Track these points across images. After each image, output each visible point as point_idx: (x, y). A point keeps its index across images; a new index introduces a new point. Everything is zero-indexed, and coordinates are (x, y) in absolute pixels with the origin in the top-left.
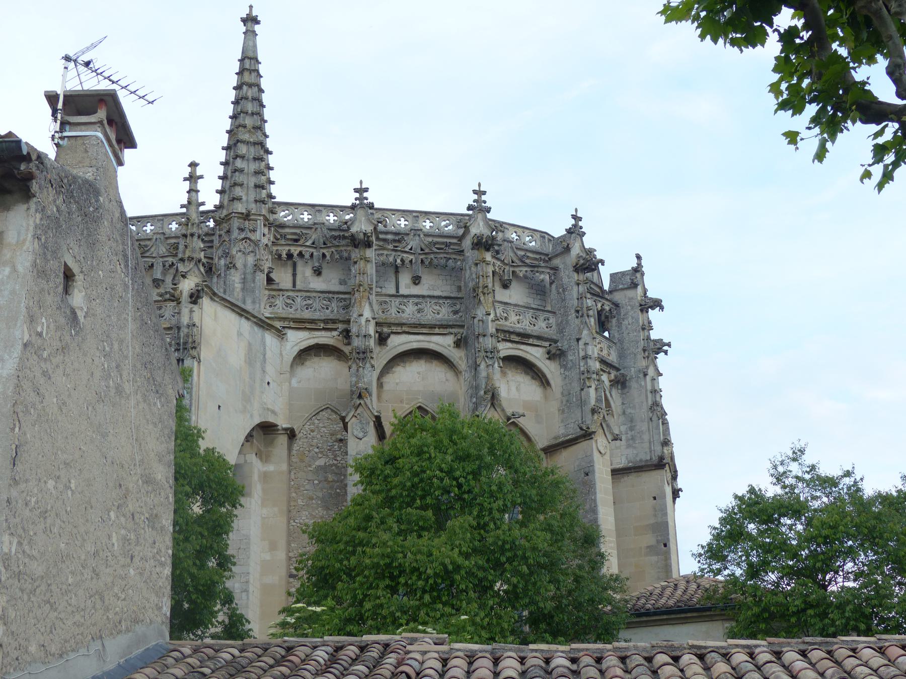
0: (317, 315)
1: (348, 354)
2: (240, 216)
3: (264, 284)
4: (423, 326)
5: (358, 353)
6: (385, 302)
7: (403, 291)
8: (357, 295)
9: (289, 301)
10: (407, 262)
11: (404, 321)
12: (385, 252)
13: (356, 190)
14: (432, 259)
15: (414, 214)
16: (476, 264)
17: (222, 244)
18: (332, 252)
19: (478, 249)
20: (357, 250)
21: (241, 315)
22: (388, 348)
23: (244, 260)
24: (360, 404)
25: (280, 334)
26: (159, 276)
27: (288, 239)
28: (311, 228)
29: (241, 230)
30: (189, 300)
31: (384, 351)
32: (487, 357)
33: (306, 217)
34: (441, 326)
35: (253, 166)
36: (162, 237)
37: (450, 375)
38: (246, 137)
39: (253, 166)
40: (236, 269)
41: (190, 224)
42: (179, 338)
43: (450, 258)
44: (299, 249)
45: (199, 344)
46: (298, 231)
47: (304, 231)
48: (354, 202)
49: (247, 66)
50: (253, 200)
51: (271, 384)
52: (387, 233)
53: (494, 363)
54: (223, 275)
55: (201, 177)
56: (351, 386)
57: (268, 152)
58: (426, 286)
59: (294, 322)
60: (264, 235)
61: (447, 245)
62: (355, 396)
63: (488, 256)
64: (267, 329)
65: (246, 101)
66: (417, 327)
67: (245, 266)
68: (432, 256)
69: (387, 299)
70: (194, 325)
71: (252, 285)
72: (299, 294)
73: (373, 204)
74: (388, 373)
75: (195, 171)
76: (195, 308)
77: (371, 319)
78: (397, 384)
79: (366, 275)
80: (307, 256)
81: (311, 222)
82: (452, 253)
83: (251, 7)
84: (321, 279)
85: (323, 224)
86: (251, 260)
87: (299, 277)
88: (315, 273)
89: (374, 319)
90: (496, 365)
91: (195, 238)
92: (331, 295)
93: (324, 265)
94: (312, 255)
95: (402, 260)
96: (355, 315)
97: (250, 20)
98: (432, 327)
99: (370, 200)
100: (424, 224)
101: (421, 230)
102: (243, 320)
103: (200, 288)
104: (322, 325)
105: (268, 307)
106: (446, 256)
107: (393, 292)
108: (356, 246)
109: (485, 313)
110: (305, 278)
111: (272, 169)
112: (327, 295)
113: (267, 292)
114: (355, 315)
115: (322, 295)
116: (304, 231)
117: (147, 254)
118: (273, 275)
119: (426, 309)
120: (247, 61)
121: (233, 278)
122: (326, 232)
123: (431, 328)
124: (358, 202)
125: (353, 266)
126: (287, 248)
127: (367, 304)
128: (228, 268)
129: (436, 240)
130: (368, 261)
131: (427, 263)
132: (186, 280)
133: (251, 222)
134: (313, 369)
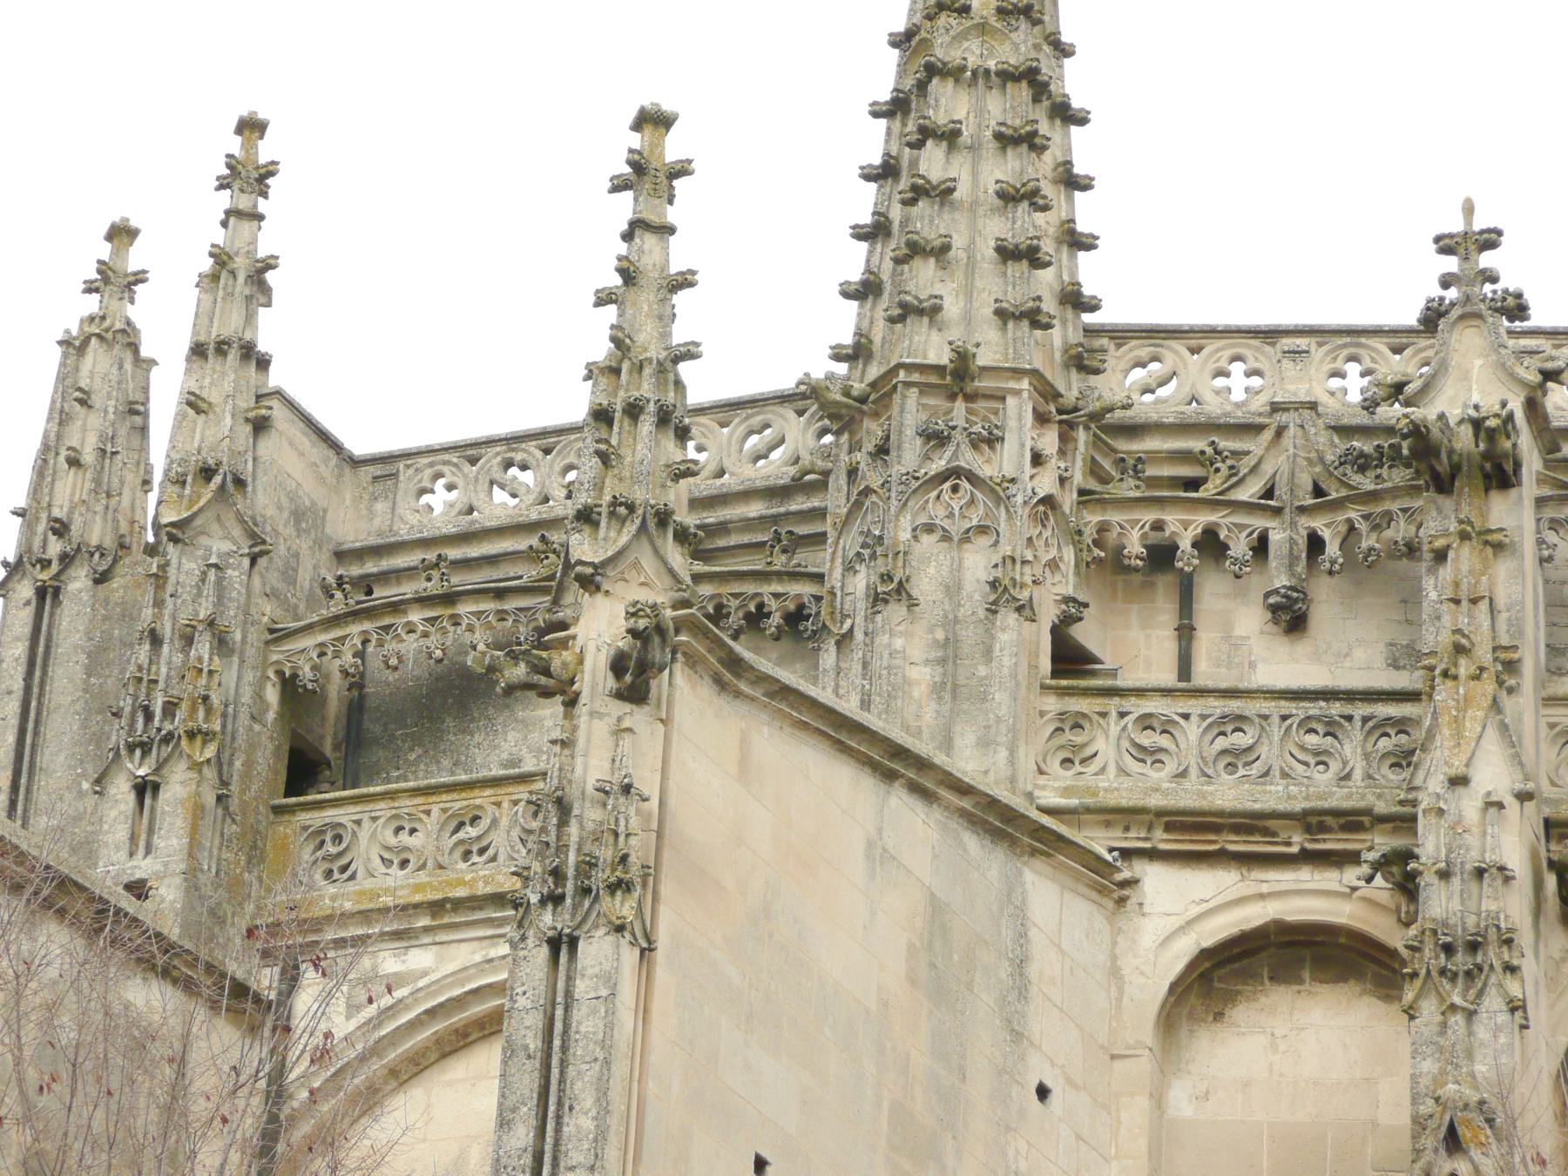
0: (1273, 796)
1: (1404, 953)
2: (933, 379)
3: (1034, 667)
5: (1448, 949)
8: (1443, 692)
9: (1147, 739)
13: (1446, 245)
17: (858, 505)
18: (1352, 528)
20: (1447, 503)
21: (889, 776)
27: (1154, 482)
29: (936, 438)
30: (611, 683)
33: (1238, 383)
38: (972, 53)
40: (912, 604)
41: (625, 367)
42: (562, 849)
44: (1204, 518)
45: (650, 874)
46: (1197, 444)
47: (1225, 444)
48: (1437, 291)
50: (988, 311)
51: (1055, 1099)
54: (859, 635)
55: (682, 170)
56: (1415, 1099)
57: (1067, 115)
59: (1168, 828)
62: (1430, 1141)
64: (1034, 852)
67: (953, 589)
70: (627, 789)
71: (982, 671)
72: (1194, 706)
73: (1519, 296)
75: (658, 145)
76: (638, 717)
77: (1509, 800)
79: (1484, 606)
80: (1240, 547)
81: (1259, 403)
84: (1303, 647)
85: (1313, 406)
86: (978, 563)
88: (1276, 621)
89: (1523, 797)
91: (647, 424)
92: (1336, 709)
94: (1261, 547)
96: (1436, 784)
99: (1508, 282)
102: (899, 800)
103: (642, 623)
104: (1298, 841)
105: (1054, 766)
108: (1443, 484)
110: (1234, 644)
111: (1083, 184)
112: (1315, 709)
113: (1052, 704)
114: (1436, 784)
115: (1299, 710)
116: (1225, 444)
118: (1086, 634)
121: (899, 643)
122: (1322, 439)
124: (1452, 294)
125: (1432, 571)
126: (1149, 516)
127: (1492, 734)
128: (877, 600)
130: (1498, 547)
132: (599, 597)
133: (980, 405)
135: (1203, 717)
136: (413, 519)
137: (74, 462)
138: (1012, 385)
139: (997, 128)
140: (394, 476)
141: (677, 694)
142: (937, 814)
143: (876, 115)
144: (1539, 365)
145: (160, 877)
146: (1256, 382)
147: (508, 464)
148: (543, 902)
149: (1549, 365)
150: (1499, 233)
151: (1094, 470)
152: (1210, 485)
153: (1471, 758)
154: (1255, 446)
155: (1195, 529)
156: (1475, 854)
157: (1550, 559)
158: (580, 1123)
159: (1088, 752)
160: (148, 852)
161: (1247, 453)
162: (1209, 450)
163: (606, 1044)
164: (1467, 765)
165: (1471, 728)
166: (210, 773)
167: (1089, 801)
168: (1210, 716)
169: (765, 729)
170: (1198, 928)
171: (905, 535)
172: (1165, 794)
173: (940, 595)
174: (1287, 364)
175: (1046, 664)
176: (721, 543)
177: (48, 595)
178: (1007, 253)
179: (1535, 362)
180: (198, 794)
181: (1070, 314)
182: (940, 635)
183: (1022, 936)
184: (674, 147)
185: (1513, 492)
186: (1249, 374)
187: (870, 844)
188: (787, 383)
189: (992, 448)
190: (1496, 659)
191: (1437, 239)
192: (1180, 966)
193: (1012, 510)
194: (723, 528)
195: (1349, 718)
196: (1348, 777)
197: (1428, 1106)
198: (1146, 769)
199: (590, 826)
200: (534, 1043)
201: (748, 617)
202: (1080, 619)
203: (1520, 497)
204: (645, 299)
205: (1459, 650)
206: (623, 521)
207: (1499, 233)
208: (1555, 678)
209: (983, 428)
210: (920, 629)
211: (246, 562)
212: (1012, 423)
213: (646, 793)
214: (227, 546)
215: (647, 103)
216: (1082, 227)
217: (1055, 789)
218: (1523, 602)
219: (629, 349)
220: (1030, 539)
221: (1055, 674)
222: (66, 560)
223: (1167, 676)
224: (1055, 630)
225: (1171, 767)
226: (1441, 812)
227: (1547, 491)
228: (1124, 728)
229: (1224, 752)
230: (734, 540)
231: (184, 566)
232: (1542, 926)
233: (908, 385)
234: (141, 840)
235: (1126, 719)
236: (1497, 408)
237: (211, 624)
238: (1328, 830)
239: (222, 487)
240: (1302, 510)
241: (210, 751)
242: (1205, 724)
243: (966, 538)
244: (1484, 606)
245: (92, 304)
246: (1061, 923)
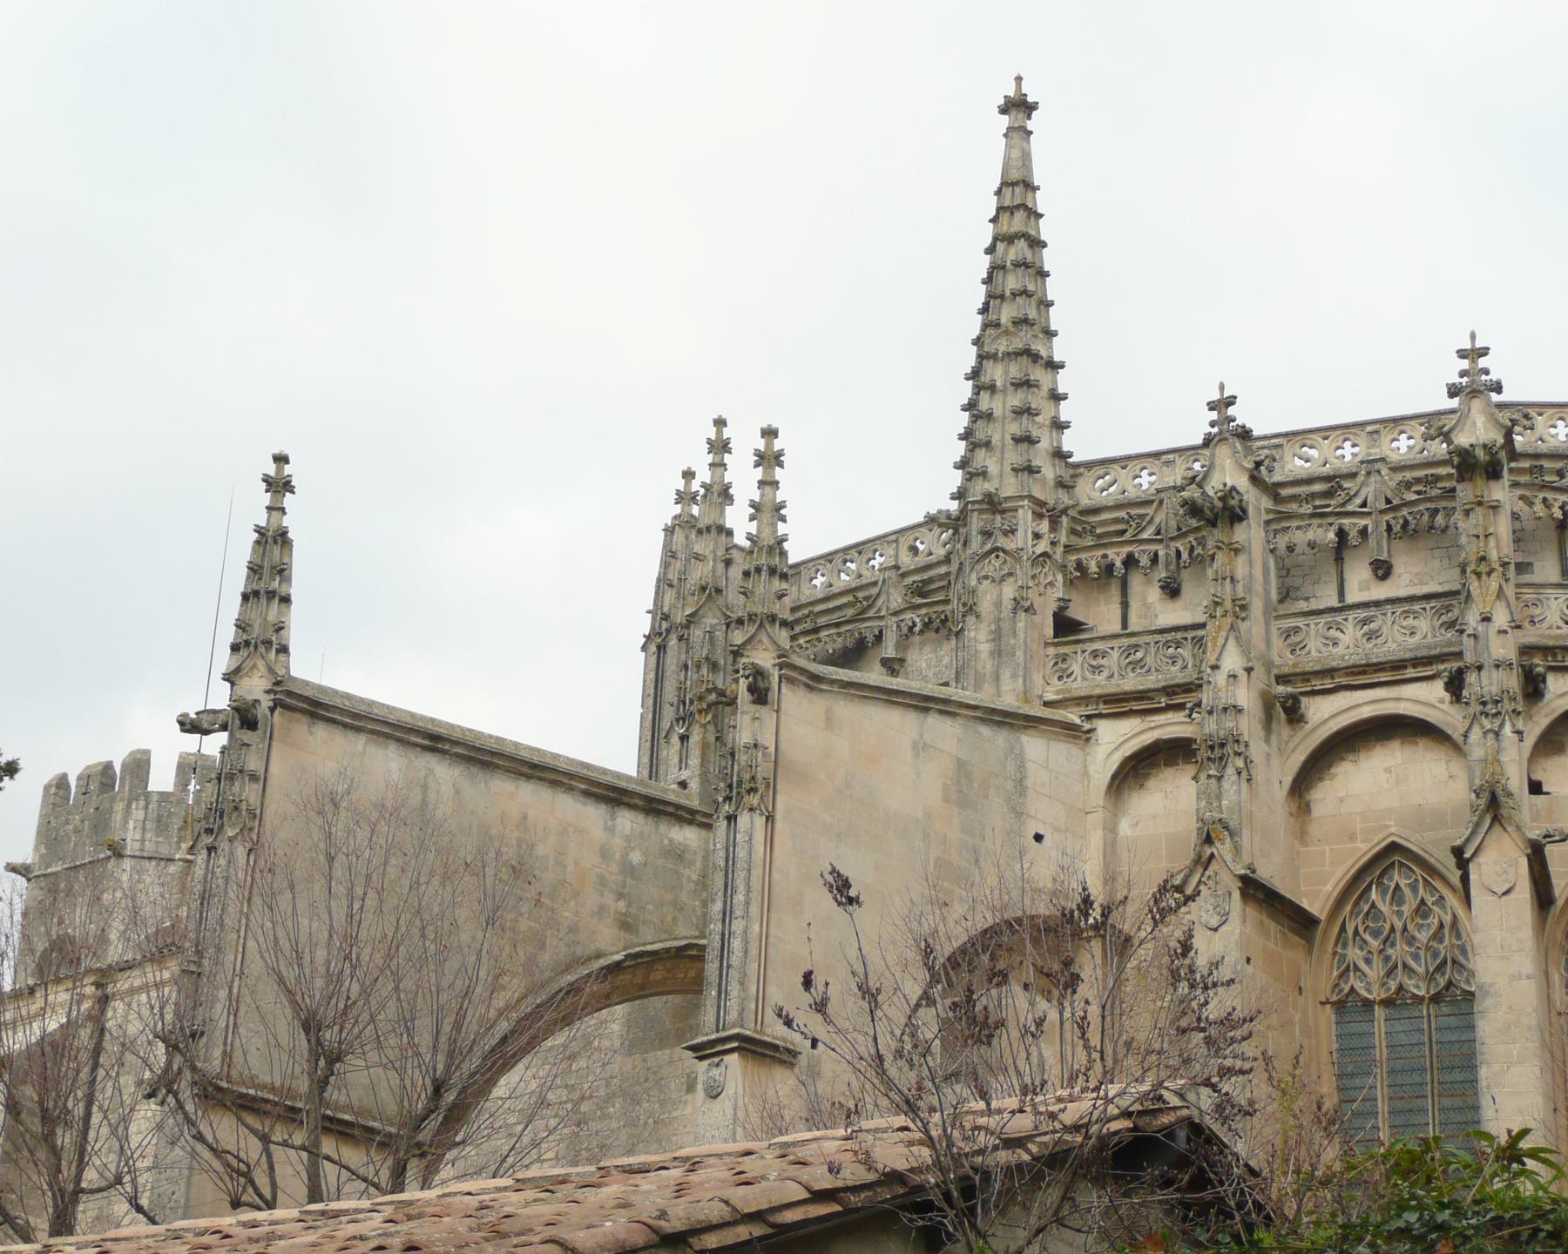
0: (1151, 681)
2: (985, 506)
4: (1379, 667)
5: (1212, 748)
6: (1297, 630)
7: (1353, 597)
10: (1353, 534)
11: (1334, 664)
12: (1295, 523)
13: (1212, 406)
14: (1406, 522)
15: (1369, 428)
16: (1467, 513)
19: (1471, 480)
20: (1215, 531)
21: (926, 710)
22: (1308, 727)
23: (993, 597)
24: (1212, 855)
25: (1079, 735)
26: (889, 650)
27: (1099, 536)
28: (1153, 501)
30: (750, 698)
31: (1300, 734)
32: (1487, 715)
33: (1145, 480)
34: (1417, 662)
35: (1016, 399)
36: (893, 574)
37: (1456, 767)
39: (1016, 399)
40: (978, 617)
43: (1436, 511)
45: (771, 785)
46: (1122, 514)
47: (1134, 512)
49: (1007, 203)
52: (1309, 481)
53: (1502, 725)
57: (1054, 366)
58: (1405, 579)
59: (1105, 703)
60: (1037, 536)
61: (1438, 478)
63: (1500, 492)
64: (1026, 727)
65: (1001, 272)
66: (1364, 672)
67: (998, 604)
68: (1405, 512)
69: (1300, 622)
70: (756, 746)
72: (1116, 643)
73: (1244, 427)
74: (1320, 780)
76: (763, 711)
78: (1341, 800)
80: (1144, 561)
81: (1153, 490)
82: (1439, 498)
83: (1019, 79)
84: (1179, 603)
86: (1009, 591)
87: (1134, 605)
90: (1508, 729)
92: (1179, 635)
93: (1185, 575)
94: (1155, 560)
95: (1341, 534)
97: (1019, 106)
98: (1399, 665)
99: (1239, 422)
100: (1395, 444)
101: (1383, 460)
102: (933, 720)
104: (1164, 701)
106: (1429, 505)
107: (1334, 603)
108: (1213, 523)
109: (1479, 618)
110: (1146, 606)
112: (1169, 637)
113: (1051, 651)
116: (1134, 512)
117: (871, 614)
118: (1076, 612)
119: (1384, 629)
120: (1008, 192)
123: (1395, 670)
124: (1215, 430)
125: (1211, 566)
126: (1099, 553)
127: (1232, 641)
129: (1409, 475)
131: (1397, 528)
134: (1162, 795)
136: (807, 592)
137: (671, 586)
138: (1021, 503)
140: (800, 573)
141: (783, 698)
142: (959, 720)
143: (967, 379)
145: (691, 778)
146: (1153, 478)
147: (845, 561)
148: (725, 800)
149: (1258, 459)
150: (1235, 397)
151: (1073, 532)
154: (1150, 511)
156: (1223, 701)
157: (1275, 549)
158: (739, 898)
159: (1069, 671)
162: (1126, 517)
163: (749, 862)
164: (1218, 659)
165: (1221, 641)
166: (711, 728)
167: (1067, 695)
169: (842, 703)
170: (1123, 747)
171: (974, 583)
173: (992, 609)
174: (1165, 468)
175: (1050, 632)
176: (932, 587)
177: (661, 649)
178: (1017, 440)
179: (1253, 458)
180: (704, 738)
181: (1057, 461)
182: (993, 627)
183: (1021, 767)
184: (778, 445)
185: (1245, 522)
186: (1151, 474)
187: (915, 745)
188: (921, 519)
191: (1208, 404)
192: (1115, 767)
194: (931, 580)
195: (1186, 639)
196: (1186, 667)
197: (1200, 824)
199: (743, 763)
200: (723, 864)
201: (942, 621)
203: (1249, 526)
204: (766, 516)
205: (1217, 604)
206: (755, 622)
207: (1235, 397)
210: (983, 626)
211: (724, 627)
212: (1021, 522)
213: (767, 744)
214: (715, 621)
215: (765, 426)
216: (1063, 418)
218: (1251, 575)
220: (1034, 577)
221: (1056, 636)
222: (668, 631)
223: (1116, 627)
224: (1056, 615)
225: (1105, 674)
226: (1209, 682)
227: (1272, 516)
229: (1130, 663)
230: (937, 585)
231: (697, 633)
232: (1274, 726)
233: (973, 511)
234: (683, 763)
236: (1221, 487)
237: (707, 659)
238: (1178, 694)
239: (710, 594)
240: (1172, 539)
241: (709, 718)
243: (1002, 580)
244: (1228, 580)
245: (678, 509)
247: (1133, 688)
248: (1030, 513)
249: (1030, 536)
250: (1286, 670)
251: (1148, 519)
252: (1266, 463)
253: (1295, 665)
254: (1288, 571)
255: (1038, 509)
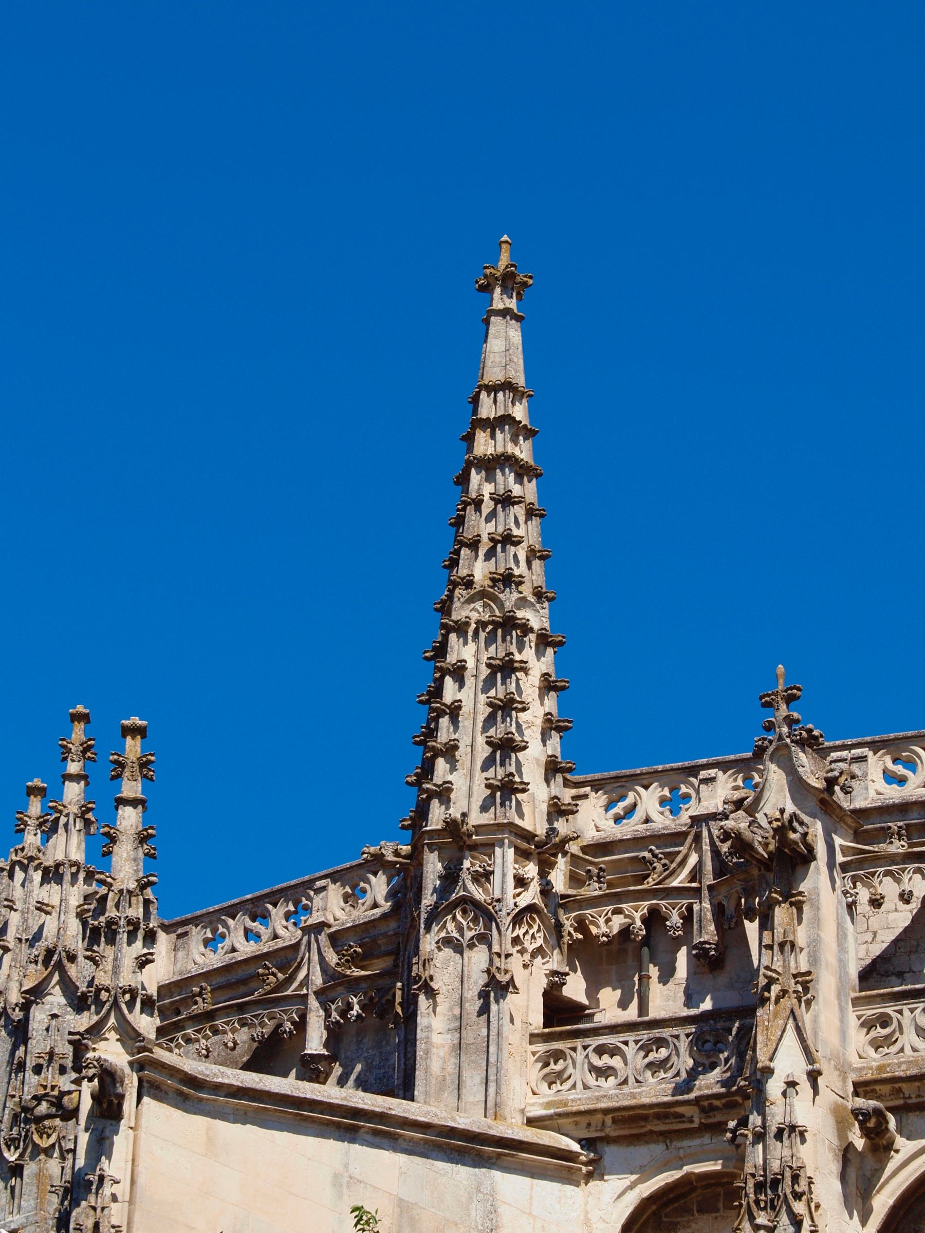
9: (606, 1060)
60: (521, 882)
72: (631, 1037)
86: (478, 958)
113: (541, 1048)
135: (636, 1042)
139: (488, 661)
144: (825, 775)
152: (650, 879)
153: (774, 1054)
155: (643, 910)
160: (19, 1211)
161: (680, 852)
168: (641, 1040)
172: (610, 1098)
175: (537, 1019)
187: (336, 1176)
189: (488, 880)
190: (796, 983)
193: (498, 920)
198: (602, 1081)
202: (565, 984)
208: (884, 978)
209: (480, 866)
213: (117, 1177)
217: (541, 1104)
219: (111, 885)
221: (544, 1027)
224: (545, 994)
228: (587, 1056)
235: (587, 1051)
236: (777, 815)
242: (638, 1046)
246: (531, 1198)
247: (654, 1100)
248: (511, 852)
249: (511, 882)
250: (869, 1076)
251: (679, 859)
252: (842, 780)
253: (881, 1068)
254: (875, 933)
255: (524, 845)
